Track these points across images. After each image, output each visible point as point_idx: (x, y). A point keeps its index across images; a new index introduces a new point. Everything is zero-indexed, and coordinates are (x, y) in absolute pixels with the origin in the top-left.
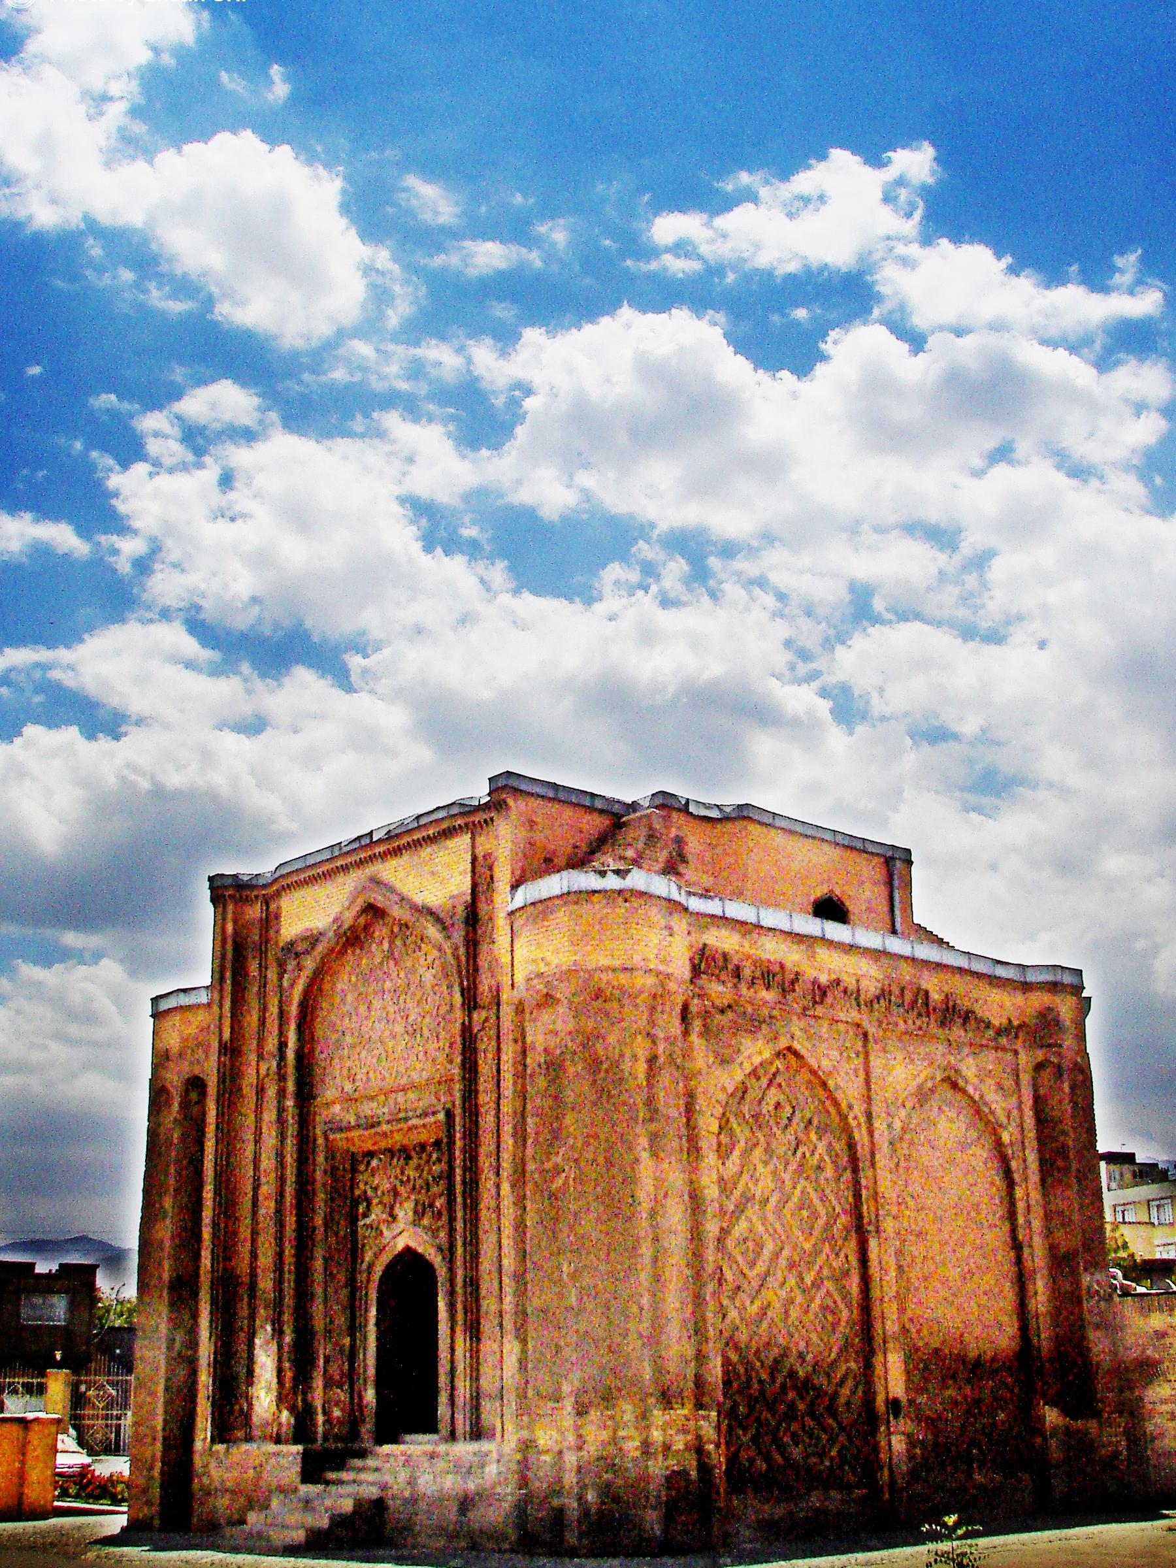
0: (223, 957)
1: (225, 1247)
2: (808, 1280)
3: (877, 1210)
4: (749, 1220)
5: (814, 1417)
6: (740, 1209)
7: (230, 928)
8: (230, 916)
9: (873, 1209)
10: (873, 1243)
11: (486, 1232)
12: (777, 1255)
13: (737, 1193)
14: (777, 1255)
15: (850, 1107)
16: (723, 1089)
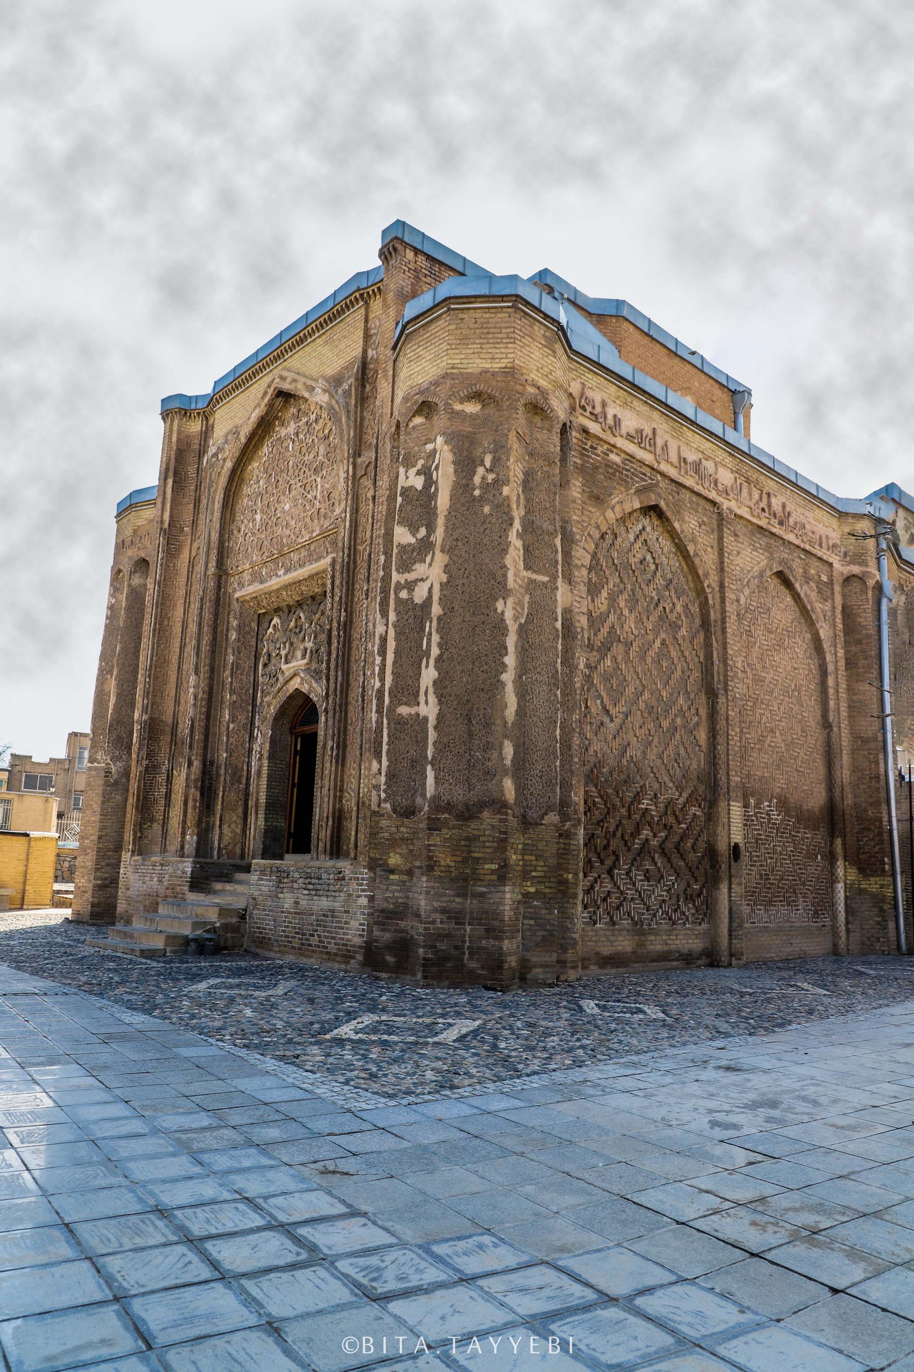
0: (168, 464)
1: (155, 693)
2: (665, 724)
3: (726, 671)
4: (614, 658)
5: (663, 853)
6: (605, 649)
7: (174, 439)
8: (175, 428)
9: (722, 671)
10: (722, 700)
11: (356, 661)
12: (639, 694)
13: (605, 631)
14: (639, 694)
15: (707, 575)
16: (598, 527)
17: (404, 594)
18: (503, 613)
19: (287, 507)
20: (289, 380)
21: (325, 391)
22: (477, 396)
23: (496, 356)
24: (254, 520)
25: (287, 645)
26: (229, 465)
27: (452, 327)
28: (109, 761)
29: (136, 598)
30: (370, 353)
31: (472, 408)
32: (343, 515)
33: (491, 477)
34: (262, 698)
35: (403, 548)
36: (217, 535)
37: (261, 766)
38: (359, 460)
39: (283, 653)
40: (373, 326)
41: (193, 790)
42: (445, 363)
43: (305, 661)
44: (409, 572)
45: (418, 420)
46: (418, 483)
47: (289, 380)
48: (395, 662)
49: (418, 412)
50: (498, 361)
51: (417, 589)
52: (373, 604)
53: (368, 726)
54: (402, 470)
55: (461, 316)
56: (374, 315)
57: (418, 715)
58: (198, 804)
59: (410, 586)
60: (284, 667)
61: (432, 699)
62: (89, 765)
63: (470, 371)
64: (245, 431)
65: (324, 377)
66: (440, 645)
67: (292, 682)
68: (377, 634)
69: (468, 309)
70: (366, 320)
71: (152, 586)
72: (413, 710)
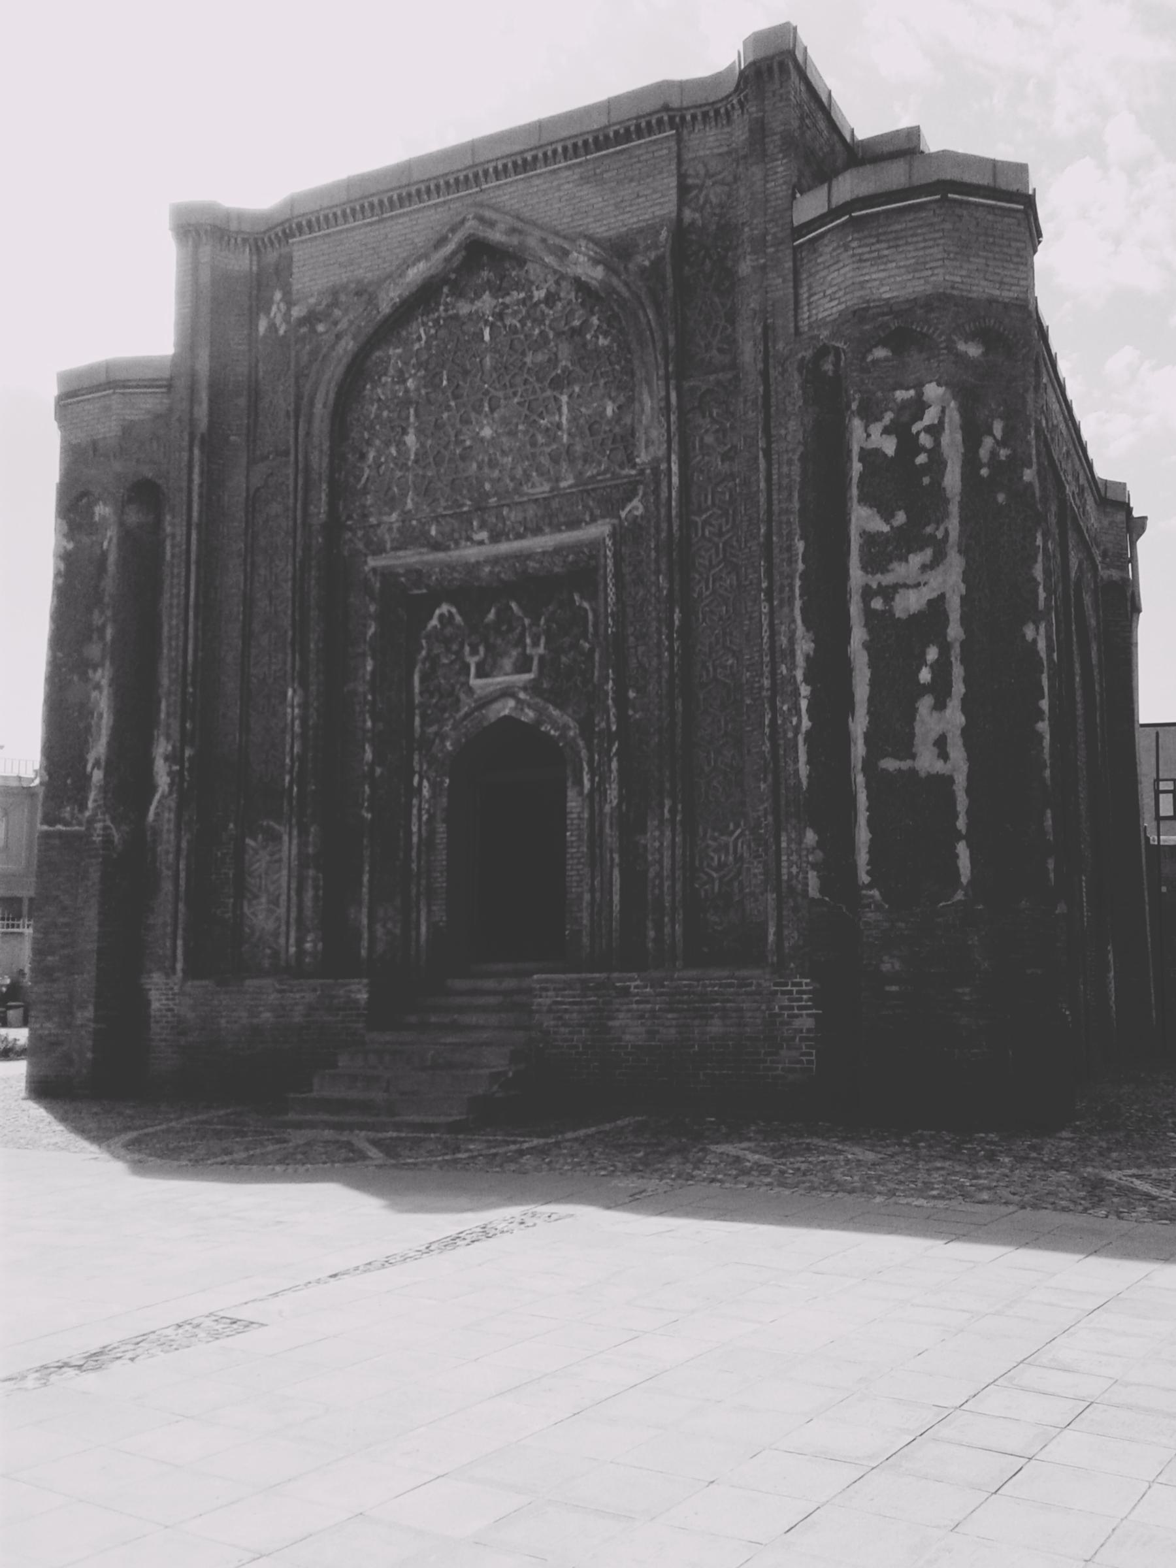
7: (205, 277)
17: (877, 604)
18: (1035, 641)
19: (487, 432)
20: (502, 226)
21: (596, 262)
22: (982, 335)
23: (1006, 280)
24: (400, 444)
25: (482, 650)
26: (348, 345)
27: (948, 226)
28: (109, 823)
29: (142, 551)
30: (688, 214)
31: (973, 350)
32: (663, 466)
33: (1003, 453)
34: (422, 725)
35: (869, 539)
36: (326, 460)
37: (432, 832)
38: (687, 385)
39: (473, 661)
40: (691, 172)
41: (311, 872)
42: (941, 278)
43: (526, 677)
44: (882, 573)
45: (880, 353)
46: (889, 446)
47: (502, 226)
48: (871, 699)
49: (884, 343)
50: (1007, 287)
51: (897, 597)
52: (786, 610)
53: (792, 782)
54: (857, 423)
55: (958, 211)
56: (691, 155)
57: (913, 772)
58: (321, 893)
59: (888, 592)
60: (474, 682)
61: (957, 753)
62: (45, 828)
63: (974, 295)
64: (390, 297)
65: (590, 238)
66: (966, 681)
67: (497, 706)
68: (799, 653)
69: (968, 203)
70: (680, 163)
71: (181, 531)
72: (905, 765)
